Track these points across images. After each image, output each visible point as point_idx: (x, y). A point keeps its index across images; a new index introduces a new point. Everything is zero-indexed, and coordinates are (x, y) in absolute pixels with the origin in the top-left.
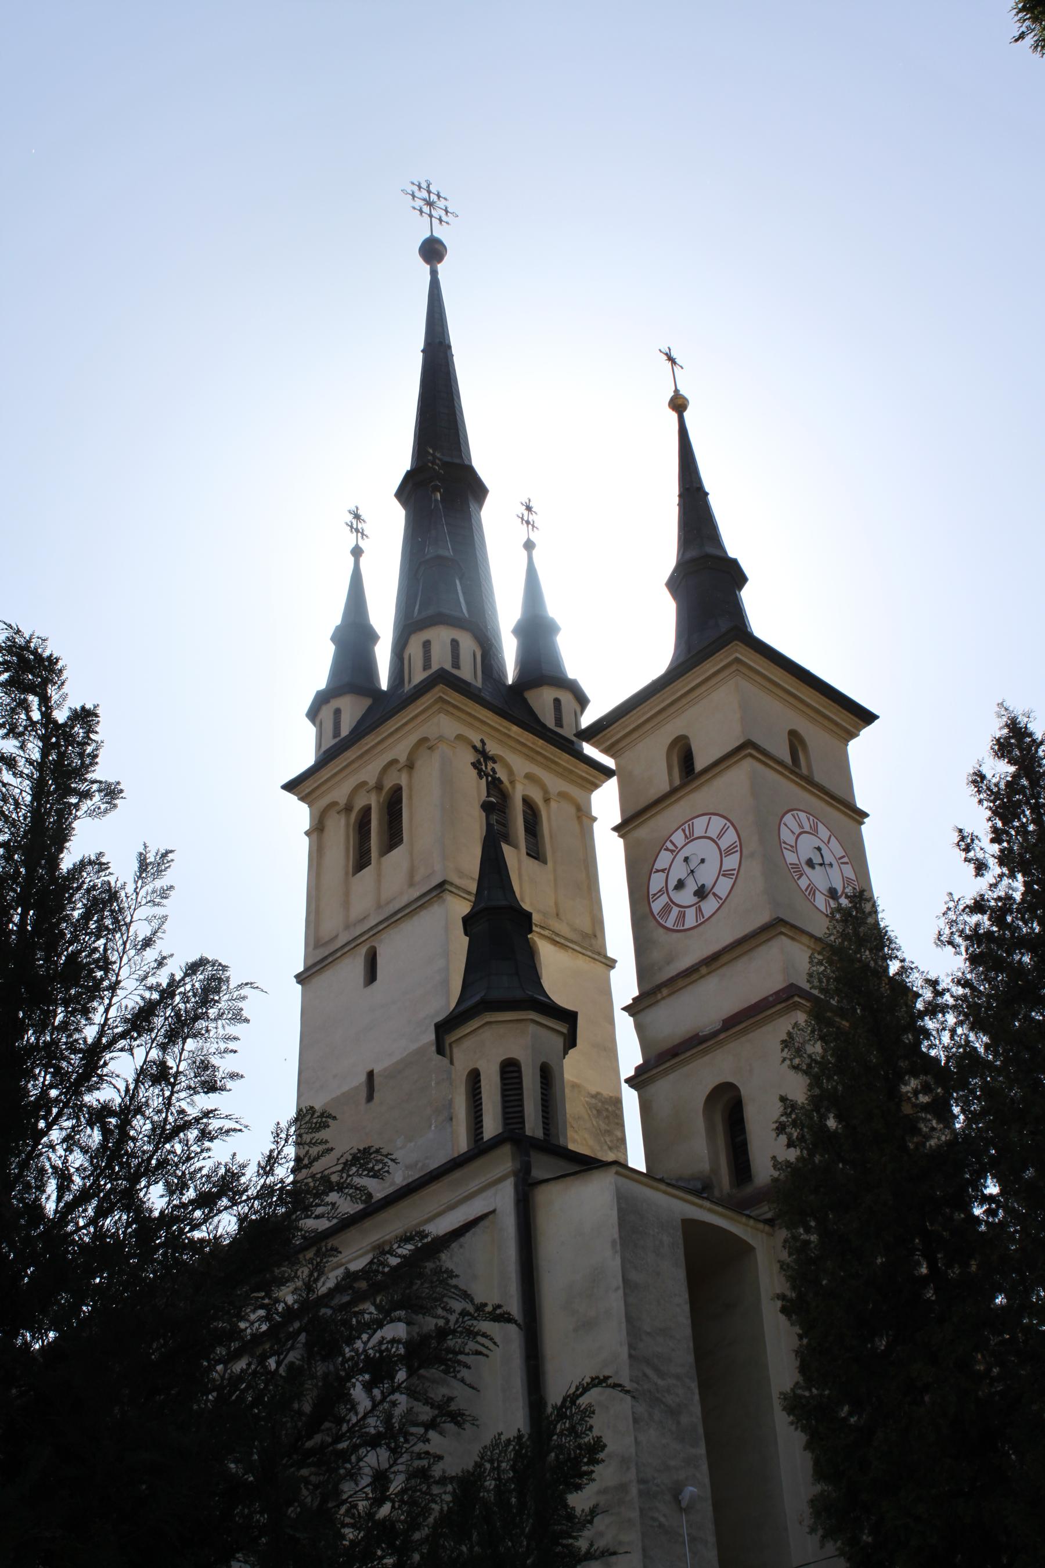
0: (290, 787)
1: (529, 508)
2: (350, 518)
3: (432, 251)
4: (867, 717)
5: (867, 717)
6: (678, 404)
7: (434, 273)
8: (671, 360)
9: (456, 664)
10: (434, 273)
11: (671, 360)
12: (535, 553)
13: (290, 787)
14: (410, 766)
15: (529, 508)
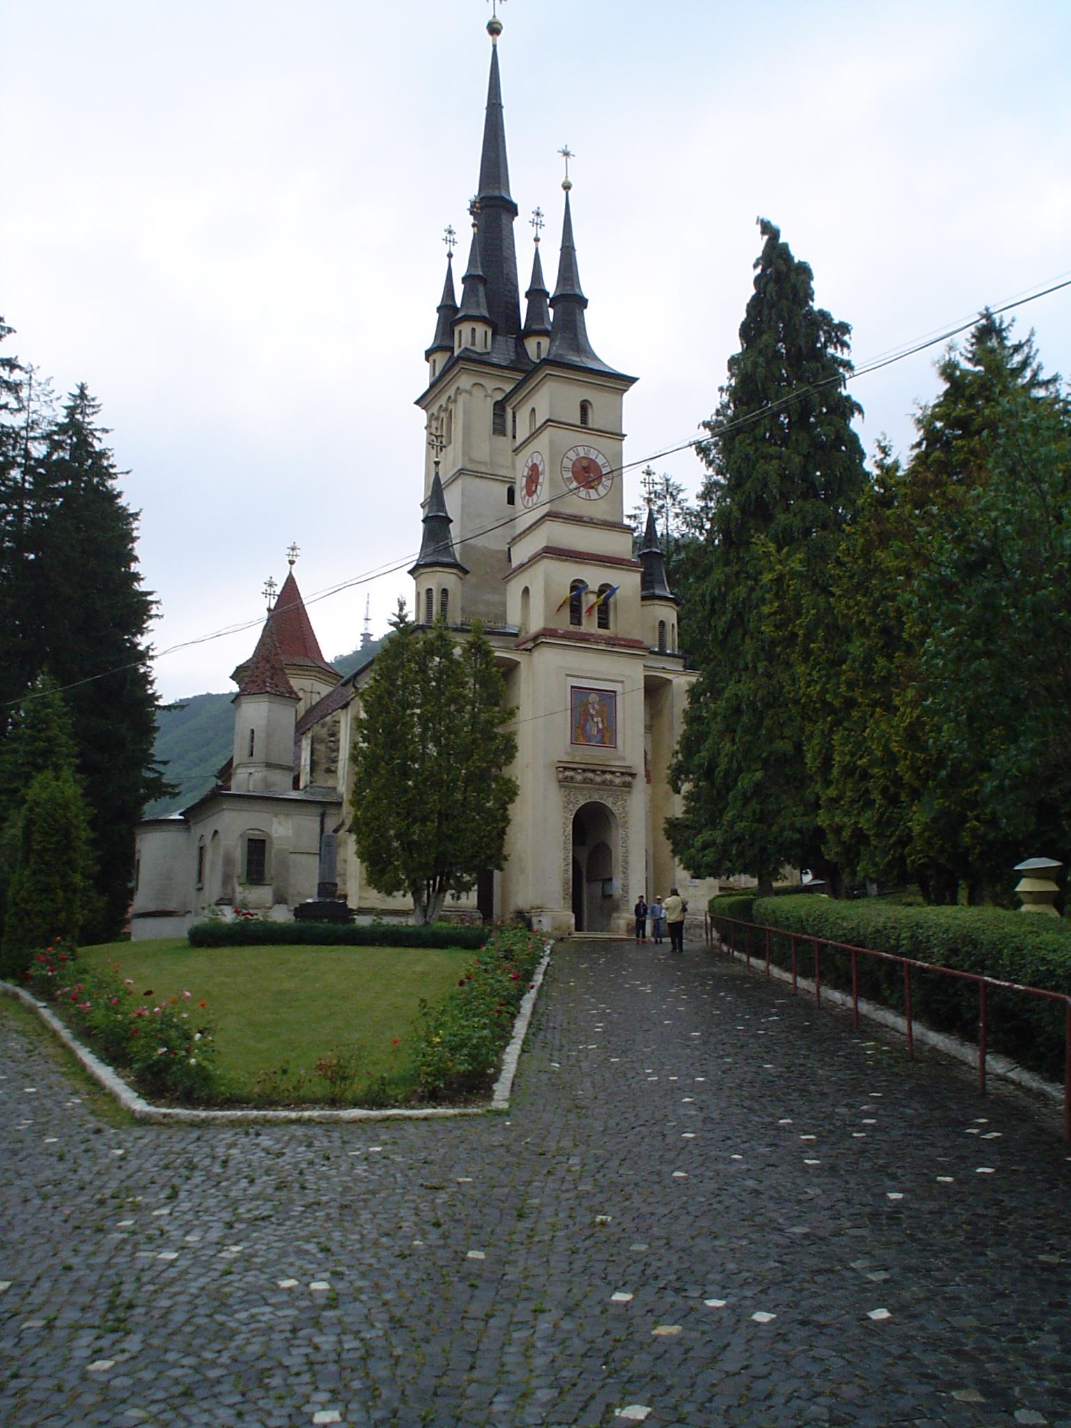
0: (417, 403)
1: (538, 214)
2: (446, 234)
3: (494, 29)
4: (633, 380)
5: (633, 380)
6: (567, 187)
7: (495, 46)
8: (566, 154)
9: (473, 344)
10: (495, 46)
11: (566, 154)
12: (540, 244)
13: (417, 403)
14: (455, 401)
15: (538, 214)
